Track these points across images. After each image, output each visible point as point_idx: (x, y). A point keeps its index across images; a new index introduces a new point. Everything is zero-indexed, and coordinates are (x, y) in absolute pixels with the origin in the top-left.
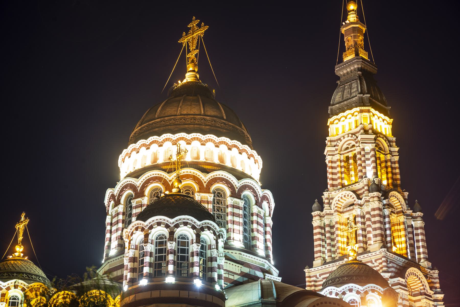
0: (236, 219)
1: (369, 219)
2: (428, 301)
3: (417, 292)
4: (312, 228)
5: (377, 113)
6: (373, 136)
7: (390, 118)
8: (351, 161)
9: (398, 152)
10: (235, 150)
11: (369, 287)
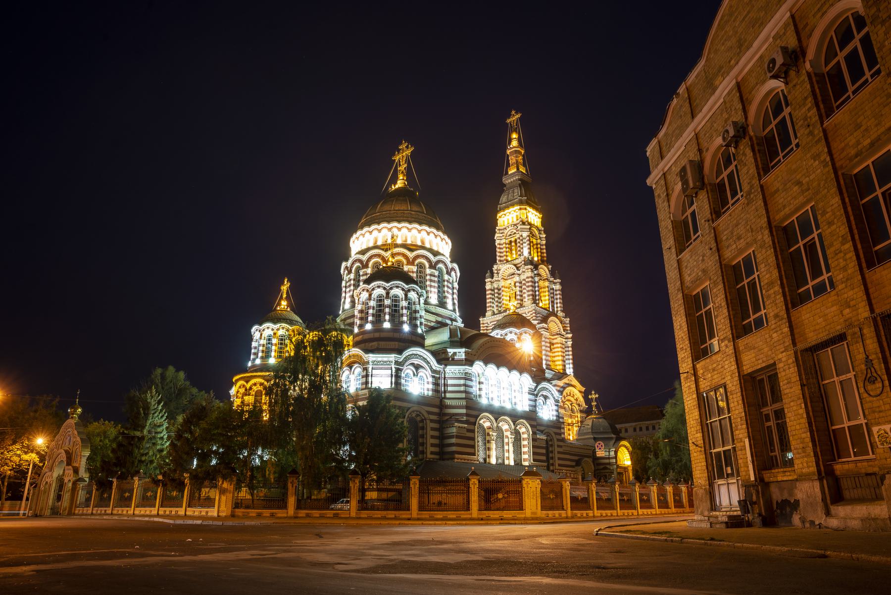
0: (433, 284)
1: (525, 284)
2: (562, 339)
4: (485, 290)
6: (529, 227)
8: (513, 244)
9: (545, 238)
10: (432, 235)
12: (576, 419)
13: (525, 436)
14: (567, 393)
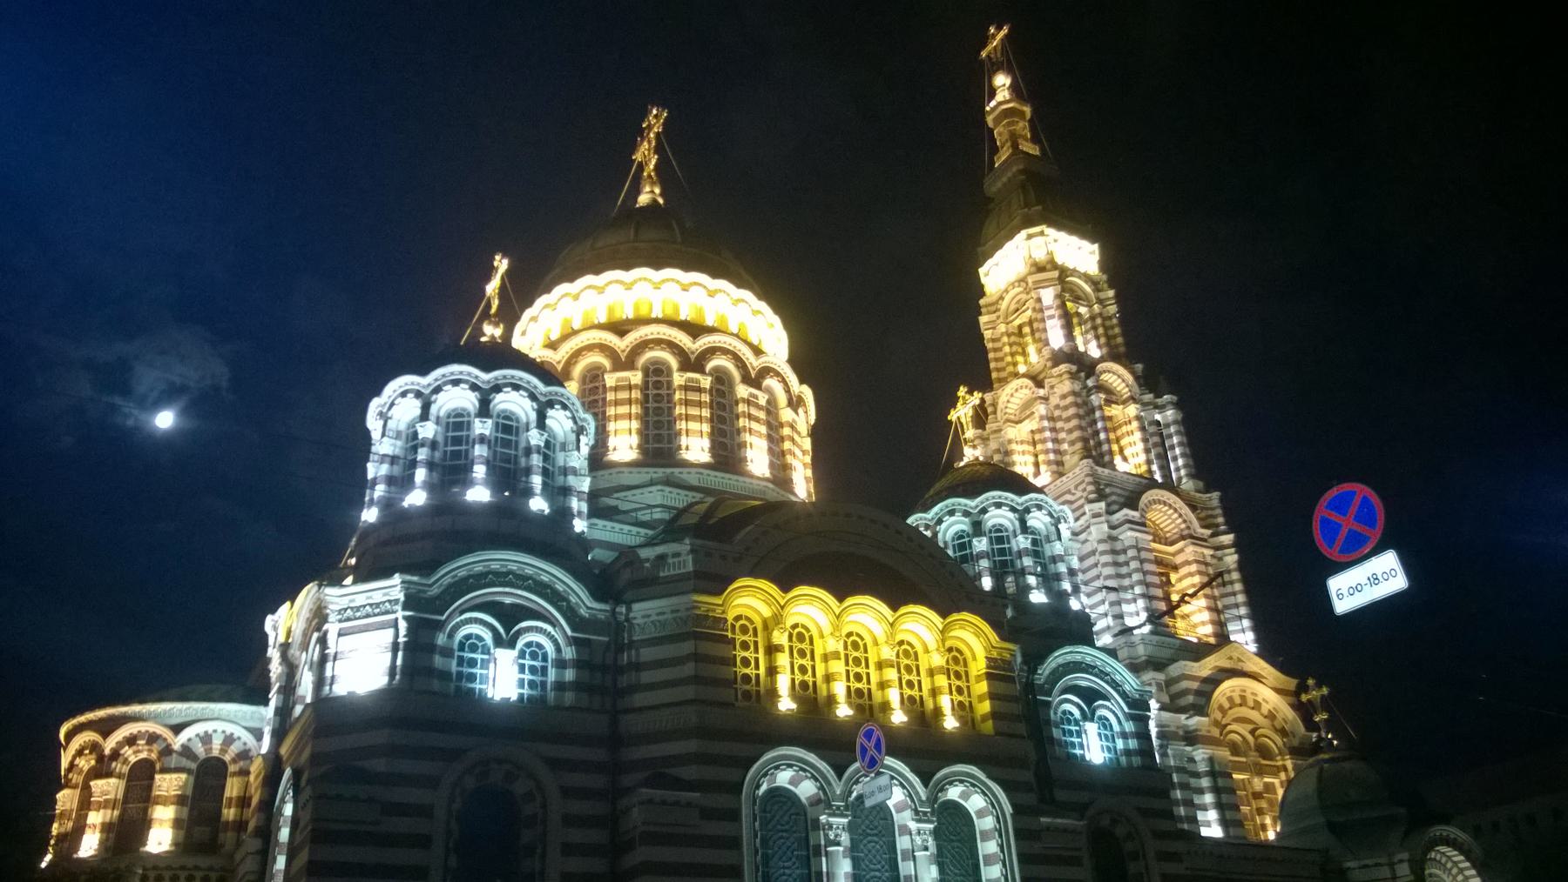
0: (694, 411)
3: (1177, 536)
6: (1056, 274)
8: (1027, 330)
11: (987, 500)
12: (1283, 776)
13: (988, 823)
14: (1230, 699)
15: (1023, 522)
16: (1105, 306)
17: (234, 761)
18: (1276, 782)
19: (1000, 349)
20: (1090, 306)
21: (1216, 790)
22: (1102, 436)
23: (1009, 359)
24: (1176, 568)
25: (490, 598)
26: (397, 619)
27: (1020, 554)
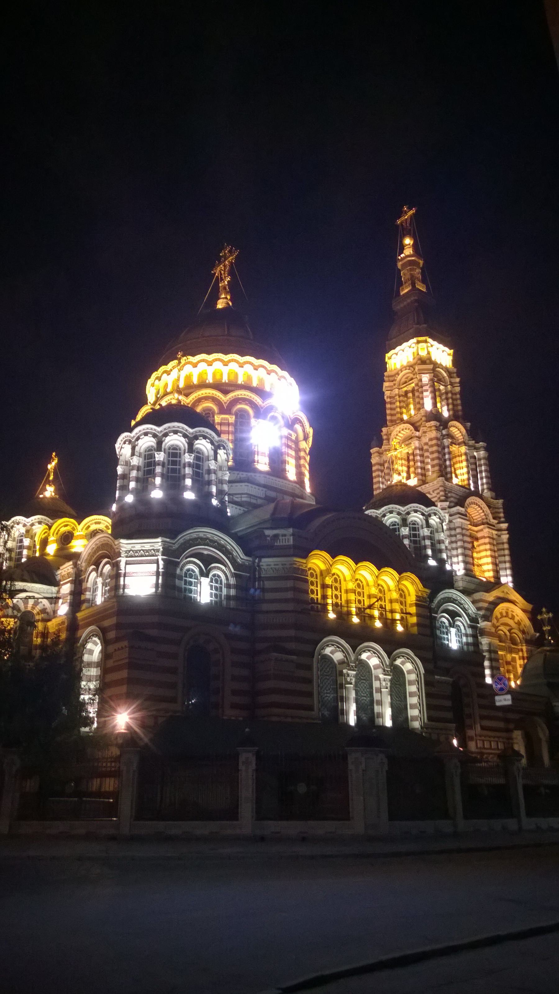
1: (427, 451)
2: (491, 531)
3: (480, 522)
4: (370, 465)
5: (435, 343)
6: (431, 367)
7: (450, 349)
8: (410, 395)
11: (411, 508)
12: (521, 654)
13: (413, 677)
14: (501, 613)
15: (427, 521)
16: (454, 387)
17: (38, 614)
18: (517, 656)
19: (394, 403)
20: (446, 386)
21: (491, 660)
22: (448, 463)
23: (398, 410)
24: (477, 539)
25: (196, 551)
26: (158, 559)
27: (424, 538)
